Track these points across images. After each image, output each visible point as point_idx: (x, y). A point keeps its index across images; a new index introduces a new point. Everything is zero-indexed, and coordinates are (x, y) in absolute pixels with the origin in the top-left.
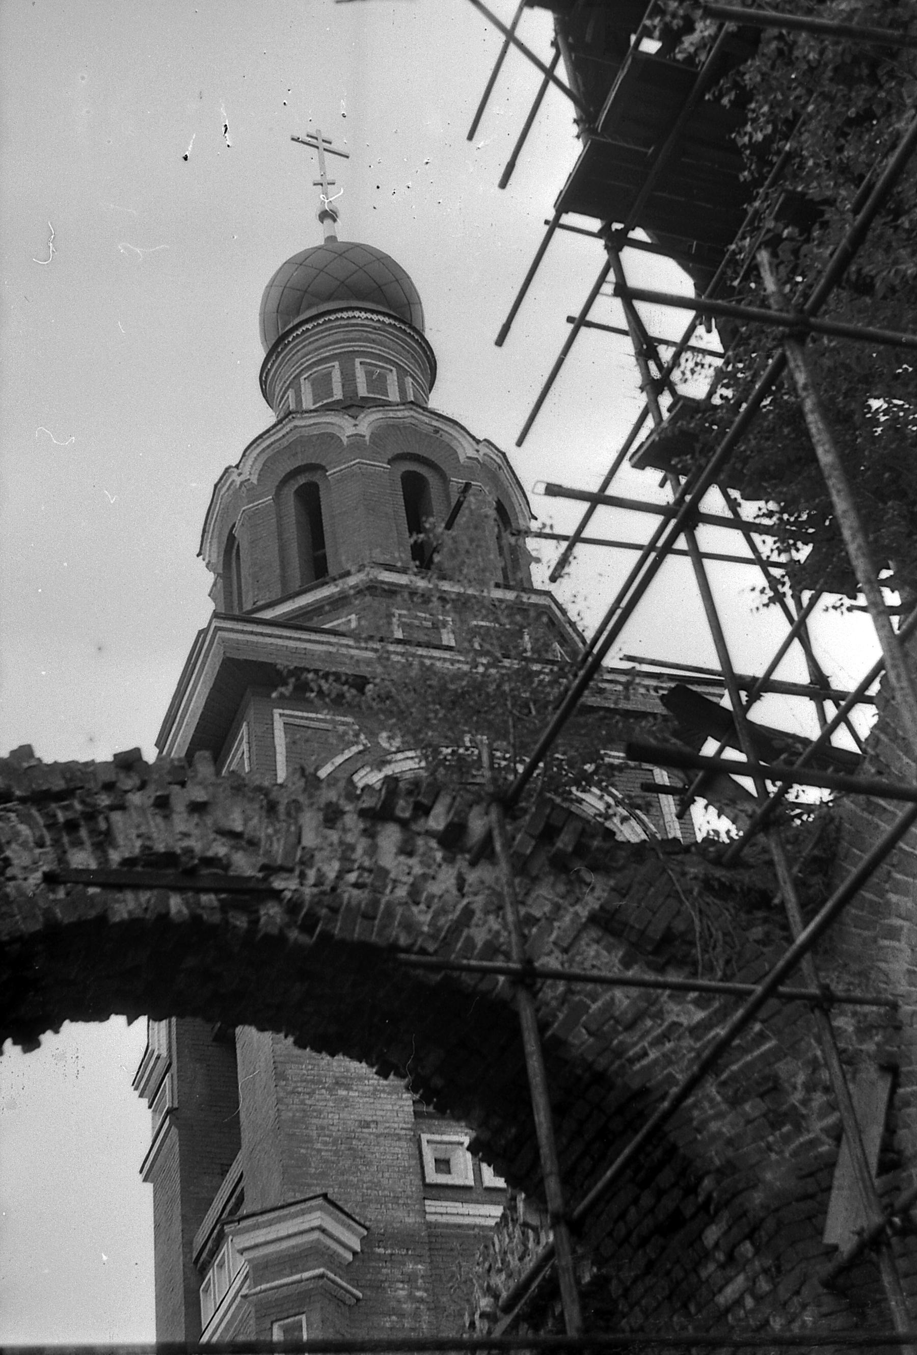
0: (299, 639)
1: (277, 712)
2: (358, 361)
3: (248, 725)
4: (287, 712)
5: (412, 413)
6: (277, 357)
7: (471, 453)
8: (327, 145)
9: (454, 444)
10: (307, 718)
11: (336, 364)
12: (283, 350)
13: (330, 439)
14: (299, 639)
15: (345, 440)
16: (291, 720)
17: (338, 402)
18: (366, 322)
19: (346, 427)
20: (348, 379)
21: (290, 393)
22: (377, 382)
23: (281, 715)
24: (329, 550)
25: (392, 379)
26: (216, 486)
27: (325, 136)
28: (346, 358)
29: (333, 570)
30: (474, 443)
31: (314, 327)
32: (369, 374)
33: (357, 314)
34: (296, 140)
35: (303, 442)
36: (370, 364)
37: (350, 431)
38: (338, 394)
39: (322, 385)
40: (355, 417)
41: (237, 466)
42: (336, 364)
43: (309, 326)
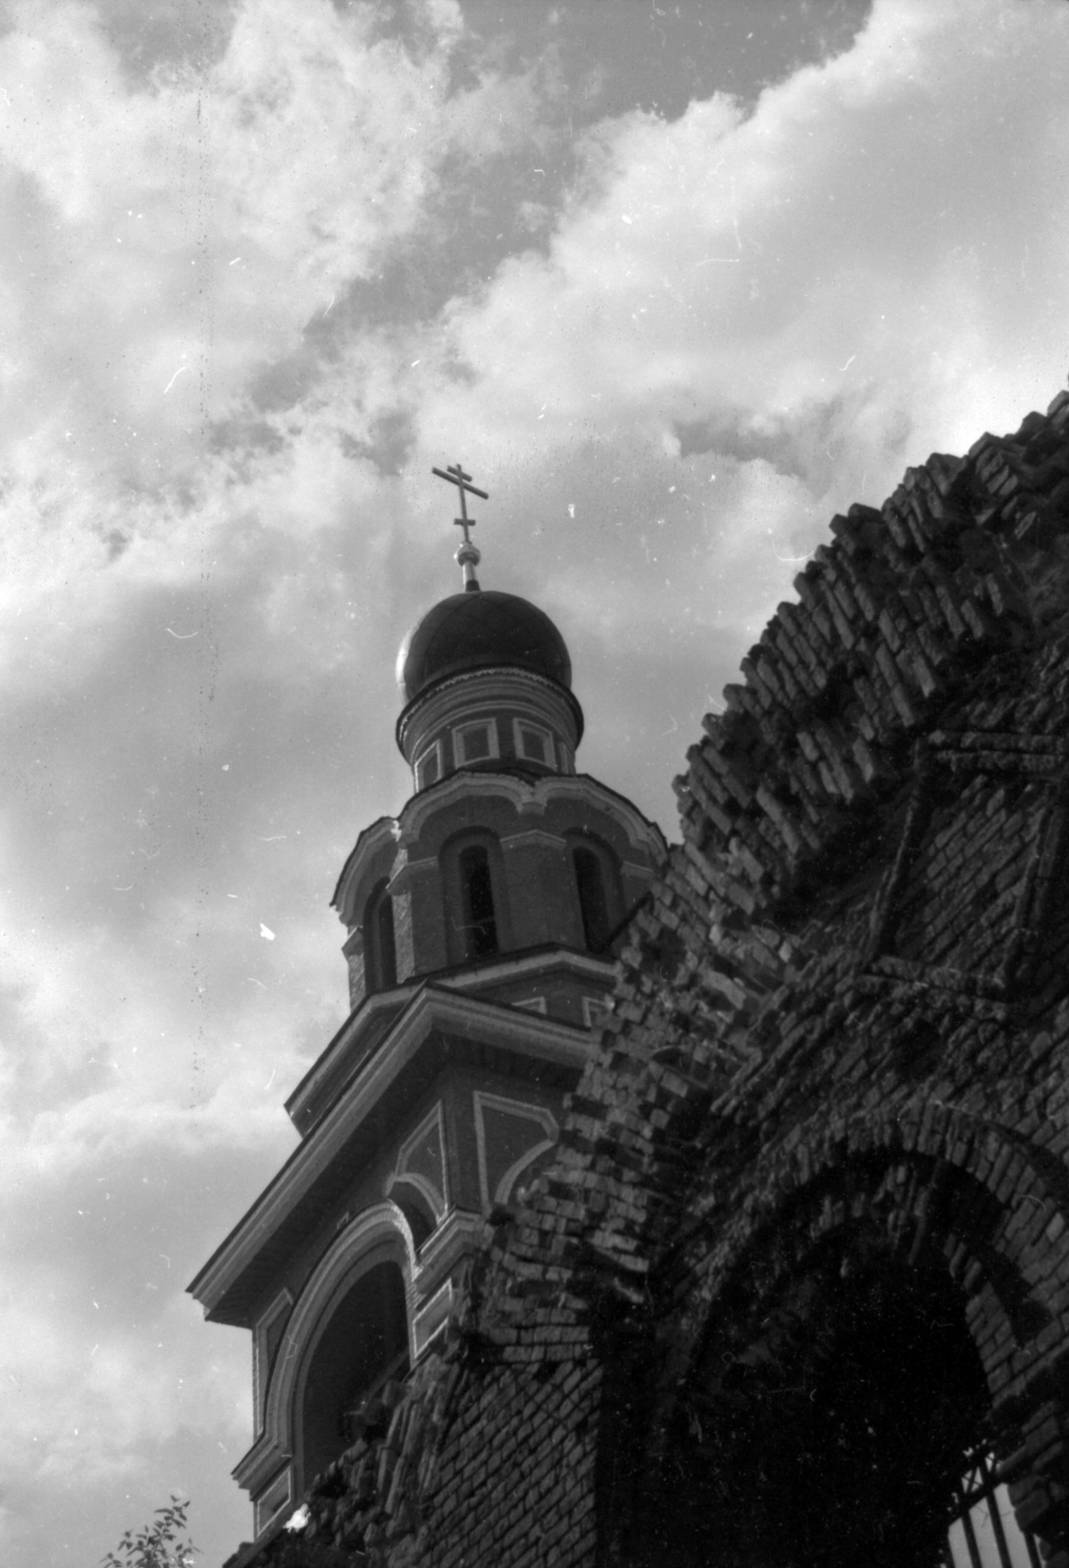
0: (507, 1020)
1: (477, 1094)
2: (516, 721)
3: (444, 1103)
4: (486, 1095)
5: (586, 787)
6: (424, 703)
7: (643, 836)
8: (465, 481)
9: (625, 824)
10: (505, 1104)
11: (493, 720)
12: (431, 697)
13: (503, 804)
14: (507, 1020)
15: (520, 808)
16: (490, 1104)
17: (493, 762)
18: (526, 681)
19: (524, 796)
20: (505, 737)
21: (437, 746)
22: (533, 744)
23: (481, 1097)
24: (499, 919)
25: (548, 744)
26: (362, 834)
27: (466, 470)
28: (504, 719)
29: (504, 943)
30: (645, 826)
31: (470, 678)
32: (525, 735)
33: (516, 671)
34: (436, 472)
35: (469, 803)
36: (528, 725)
37: (526, 798)
38: (494, 752)
39: (476, 742)
40: (532, 785)
41: (399, 819)
42: (493, 720)
43: (466, 677)
